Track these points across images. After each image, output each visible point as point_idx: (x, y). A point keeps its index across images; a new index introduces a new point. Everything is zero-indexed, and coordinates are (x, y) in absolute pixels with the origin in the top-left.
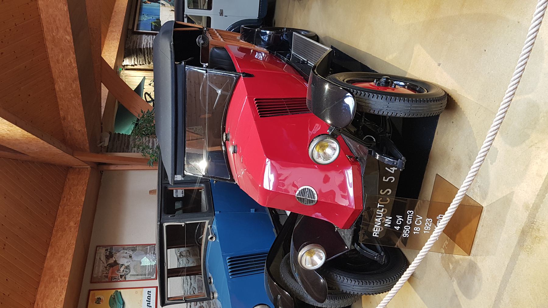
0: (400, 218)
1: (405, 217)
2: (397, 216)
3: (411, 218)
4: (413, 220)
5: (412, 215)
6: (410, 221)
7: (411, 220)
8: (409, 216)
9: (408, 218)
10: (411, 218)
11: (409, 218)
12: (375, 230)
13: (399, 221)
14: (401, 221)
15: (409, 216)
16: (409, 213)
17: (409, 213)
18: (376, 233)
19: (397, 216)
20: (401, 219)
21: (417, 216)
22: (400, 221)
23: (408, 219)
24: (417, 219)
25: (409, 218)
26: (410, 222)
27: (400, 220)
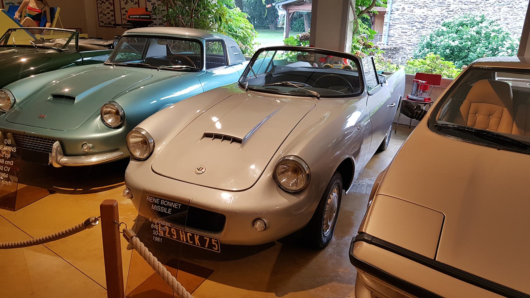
12: (151, 199)
18: (149, 199)
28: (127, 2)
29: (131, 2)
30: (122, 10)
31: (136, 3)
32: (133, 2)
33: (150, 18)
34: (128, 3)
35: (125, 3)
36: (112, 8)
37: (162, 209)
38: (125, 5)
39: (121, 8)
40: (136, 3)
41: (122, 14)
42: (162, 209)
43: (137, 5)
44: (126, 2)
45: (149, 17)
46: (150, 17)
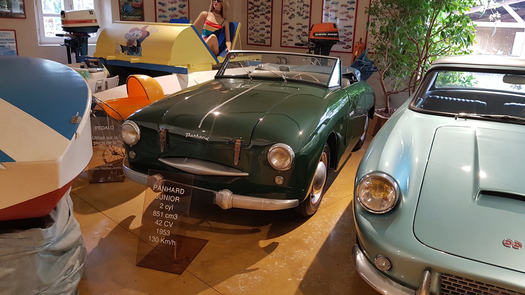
1: (171, 212)
2: (173, 205)
13: (168, 207)
20: (170, 209)
22: (168, 208)
27: (169, 209)
28: (293, 16)
29: (299, 16)
30: (283, 26)
31: (307, 17)
32: (302, 17)
33: (337, 36)
34: (294, 17)
35: (289, 17)
36: (268, 23)
38: (290, 19)
39: (283, 23)
40: (307, 17)
41: (283, 31)
43: (308, 20)
44: (291, 16)
45: (336, 34)
46: (338, 35)
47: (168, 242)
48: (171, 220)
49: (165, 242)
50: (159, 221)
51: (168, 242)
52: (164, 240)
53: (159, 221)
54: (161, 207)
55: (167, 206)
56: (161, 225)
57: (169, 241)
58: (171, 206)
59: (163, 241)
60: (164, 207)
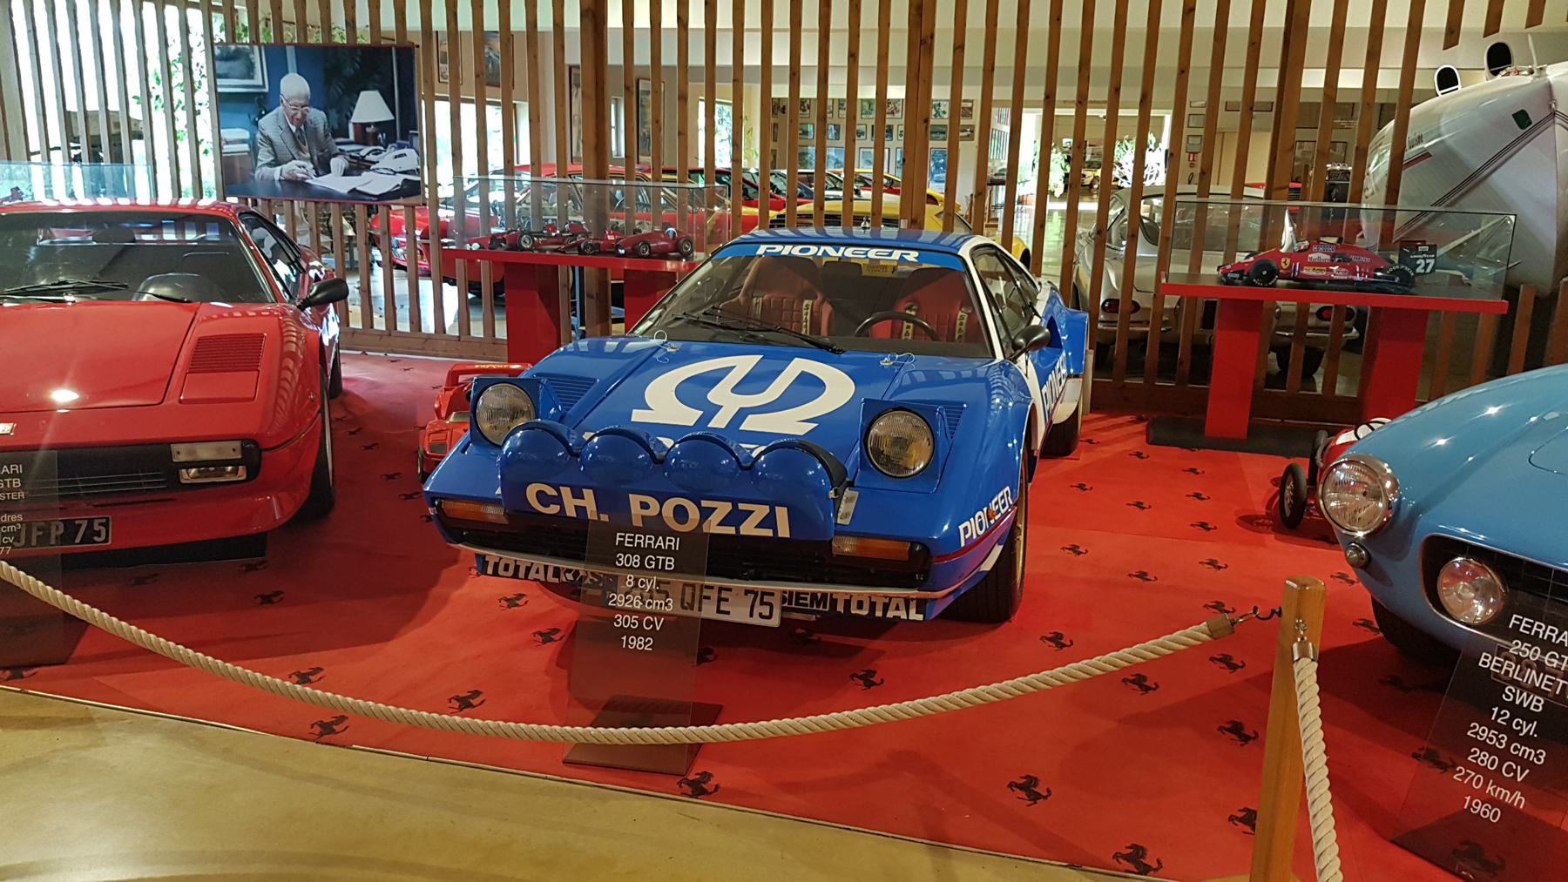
0: (1529, 728)
1: (1527, 741)
2: (1535, 723)
3: (1526, 757)
4: (1518, 760)
5: (1531, 759)
6: (1517, 752)
7: (1520, 755)
8: (1530, 753)
9: (1527, 748)
10: (1526, 757)
11: (1525, 751)
13: (1522, 725)
14: (1521, 731)
15: (1530, 753)
16: (1538, 752)
17: (1538, 752)
19: (1535, 723)
20: (1525, 731)
21: (1527, 771)
22: (1519, 728)
23: (1523, 748)
24: (1519, 768)
25: (1525, 751)
26: (1514, 750)
37: (1509, 693)
42: (1509, 693)
47: (1506, 794)
48: (1524, 763)
49: (1494, 794)
50: (1502, 713)
51: (1506, 794)
52: (1495, 790)
53: (1502, 713)
54: (1502, 720)
55: (1518, 722)
56: (1504, 723)
57: (1509, 793)
58: (1530, 725)
59: (1492, 791)
60: (1509, 721)
